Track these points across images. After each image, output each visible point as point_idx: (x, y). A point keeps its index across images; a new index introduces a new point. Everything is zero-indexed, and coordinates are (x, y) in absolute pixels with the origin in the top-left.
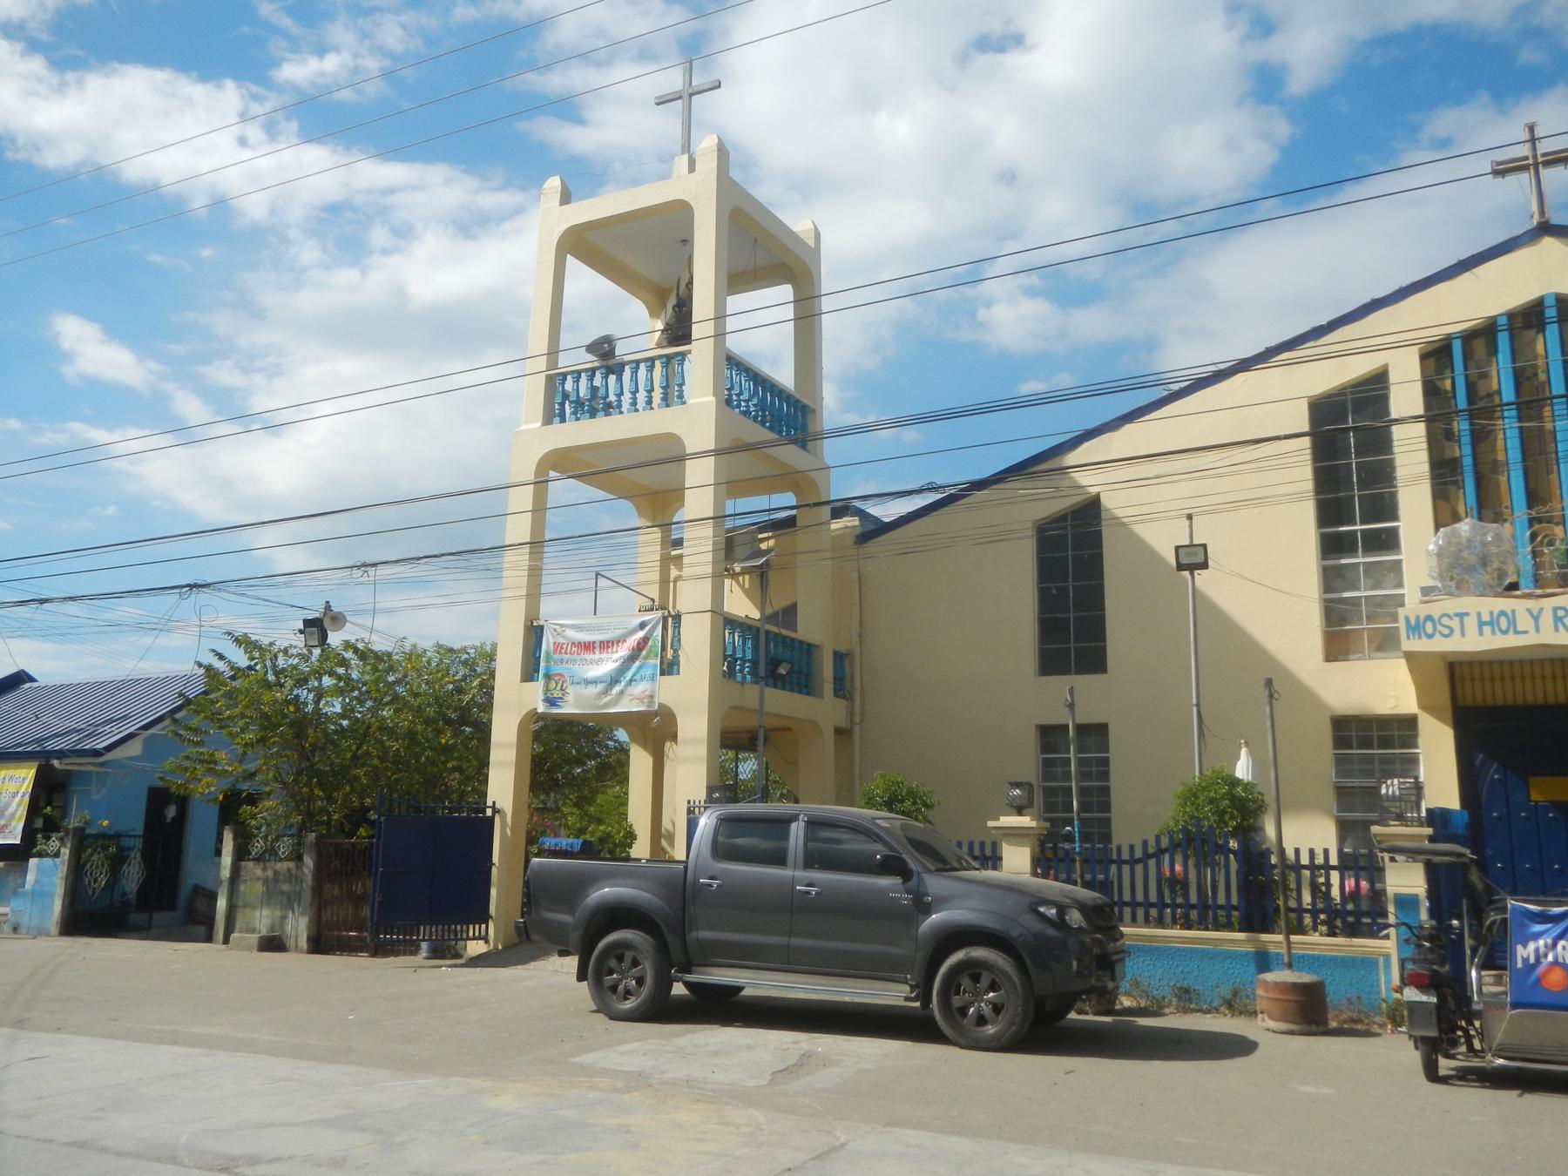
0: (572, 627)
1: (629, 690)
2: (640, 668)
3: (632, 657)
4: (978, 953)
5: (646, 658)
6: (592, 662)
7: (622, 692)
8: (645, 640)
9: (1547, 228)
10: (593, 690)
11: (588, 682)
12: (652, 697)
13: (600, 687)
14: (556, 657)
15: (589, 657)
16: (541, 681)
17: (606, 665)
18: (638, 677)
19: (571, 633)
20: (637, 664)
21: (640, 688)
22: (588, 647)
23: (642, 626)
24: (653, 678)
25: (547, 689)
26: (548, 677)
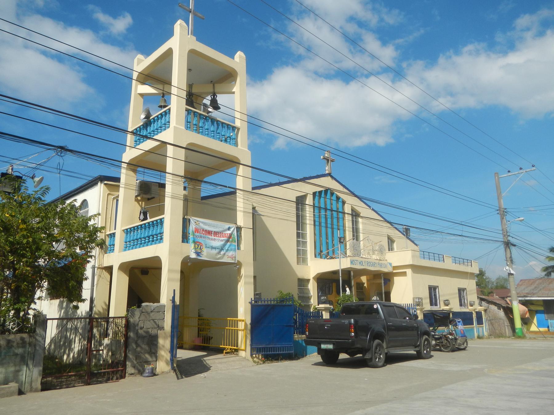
0: (202, 223)
1: (227, 254)
2: (230, 245)
3: (227, 241)
4: (427, 337)
5: (232, 242)
6: (212, 239)
7: (224, 254)
8: (230, 236)
9: (329, 175)
10: (214, 252)
11: (213, 248)
12: (235, 257)
13: (217, 251)
14: (197, 234)
15: (210, 237)
16: (192, 245)
17: (218, 242)
18: (229, 249)
19: (201, 225)
20: (229, 244)
21: (231, 253)
22: (209, 233)
23: (229, 229)
24: (235, 250)
25: (195, 248)
26: (195, 242)
